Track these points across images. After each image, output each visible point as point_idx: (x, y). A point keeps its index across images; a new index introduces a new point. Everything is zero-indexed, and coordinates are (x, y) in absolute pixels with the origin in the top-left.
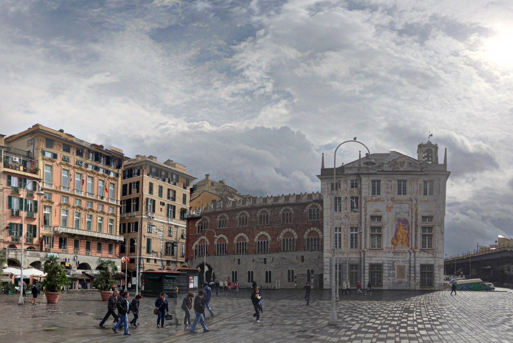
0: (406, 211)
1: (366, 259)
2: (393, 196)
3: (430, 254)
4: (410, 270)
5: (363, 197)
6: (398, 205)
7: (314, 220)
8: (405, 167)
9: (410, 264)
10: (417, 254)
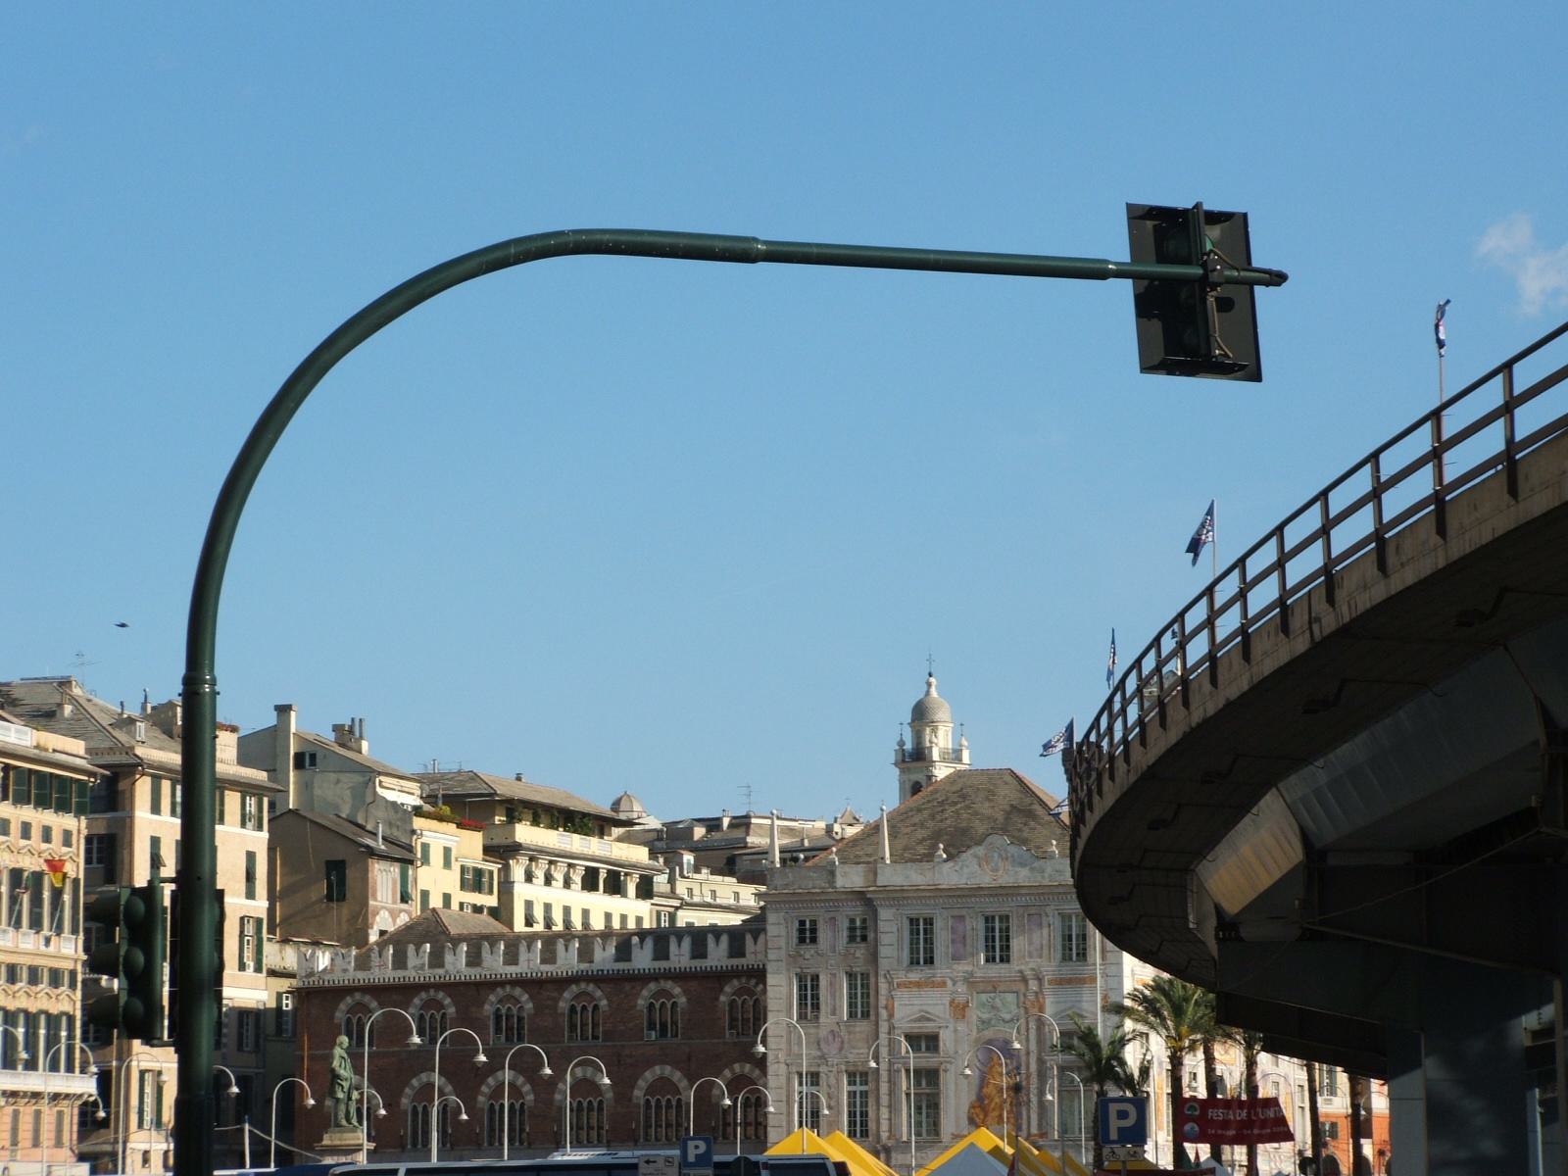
0: (1007, 1017)
2: (969, 968)
6: (984, 997)
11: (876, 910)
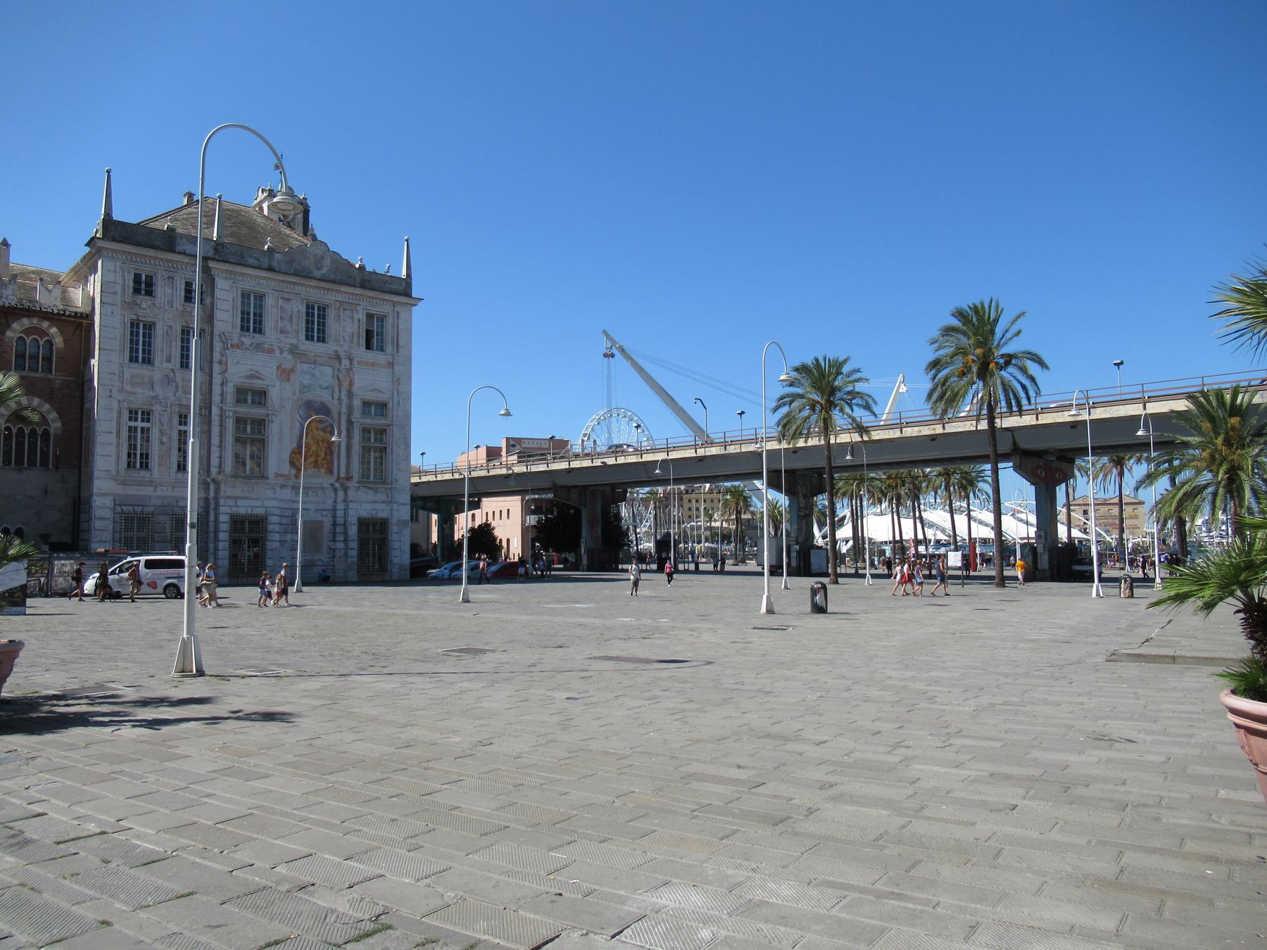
0: (325, 385)
1: (222, 502)
2: (295, 342)
3: (379, 494)
4: (334, 534)
5: (216, 332)
6: (306, 366)
7: (33, 375)
8: (324, 271)
9: (334, 517)
10: (350, 492)
11: (214, 279)
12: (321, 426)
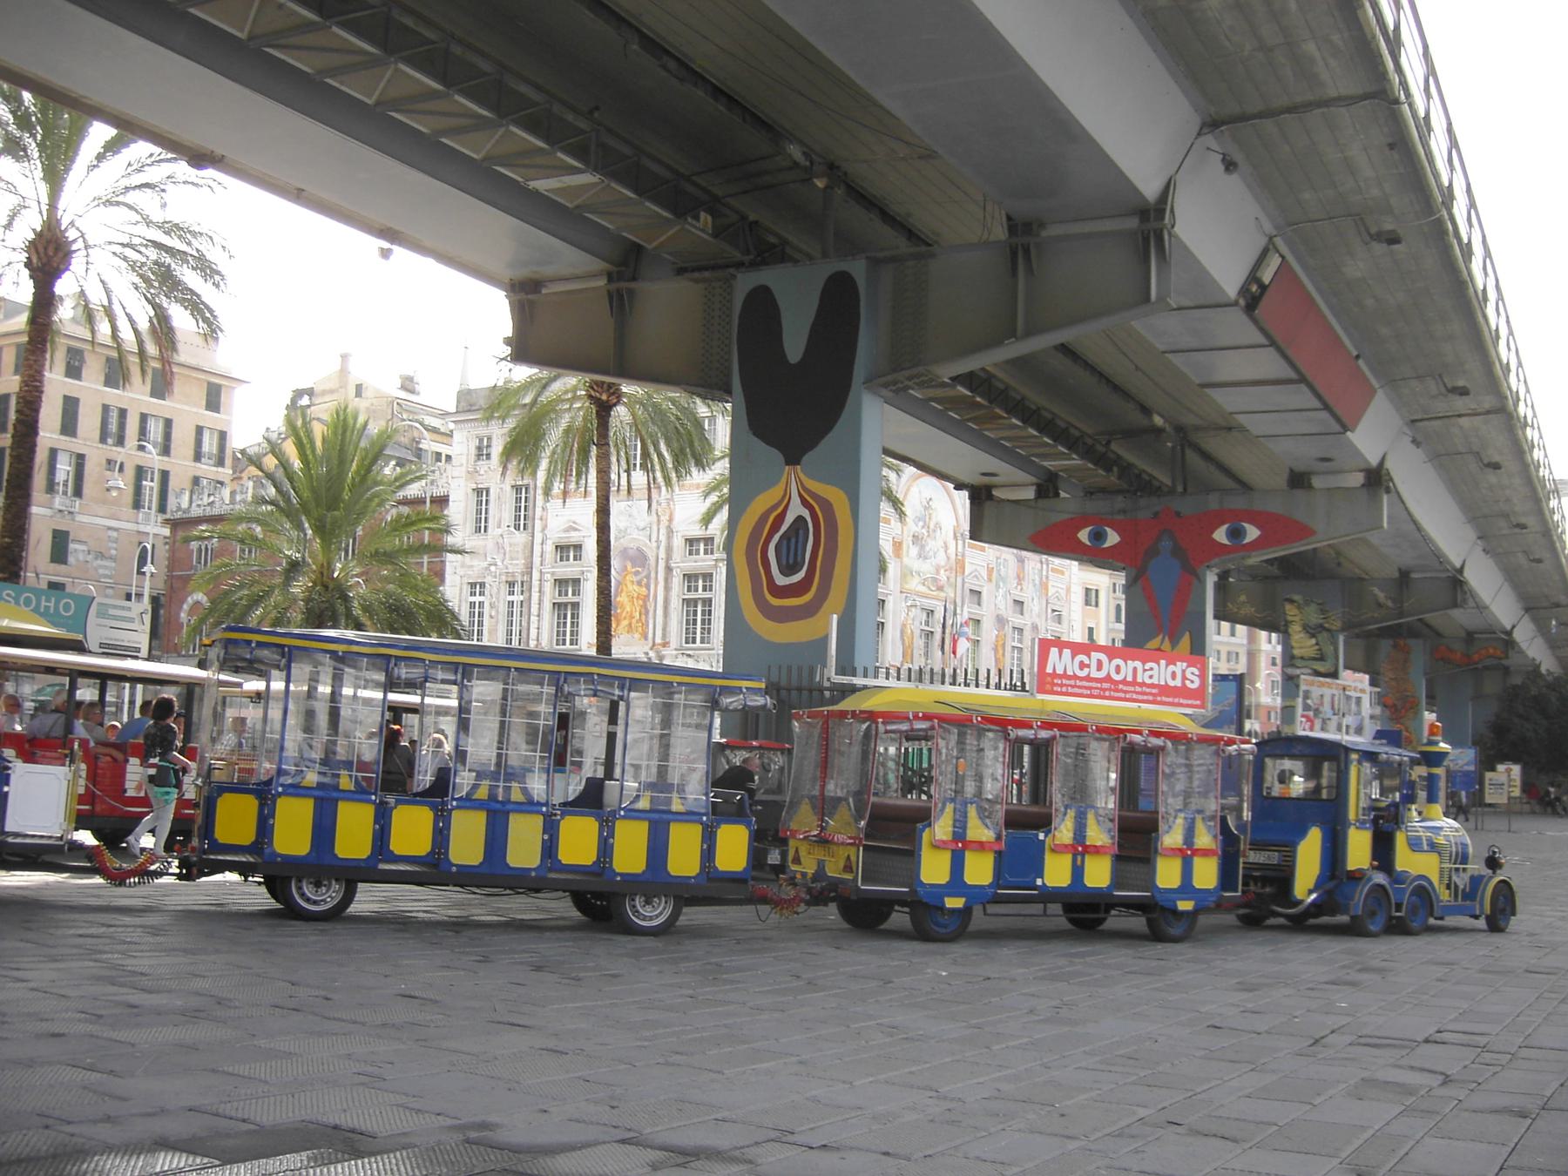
0: (642, 525)
12: (635, 579)
